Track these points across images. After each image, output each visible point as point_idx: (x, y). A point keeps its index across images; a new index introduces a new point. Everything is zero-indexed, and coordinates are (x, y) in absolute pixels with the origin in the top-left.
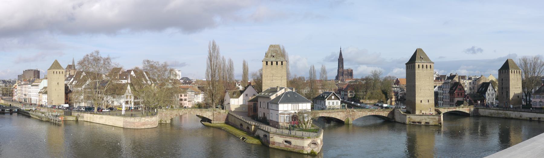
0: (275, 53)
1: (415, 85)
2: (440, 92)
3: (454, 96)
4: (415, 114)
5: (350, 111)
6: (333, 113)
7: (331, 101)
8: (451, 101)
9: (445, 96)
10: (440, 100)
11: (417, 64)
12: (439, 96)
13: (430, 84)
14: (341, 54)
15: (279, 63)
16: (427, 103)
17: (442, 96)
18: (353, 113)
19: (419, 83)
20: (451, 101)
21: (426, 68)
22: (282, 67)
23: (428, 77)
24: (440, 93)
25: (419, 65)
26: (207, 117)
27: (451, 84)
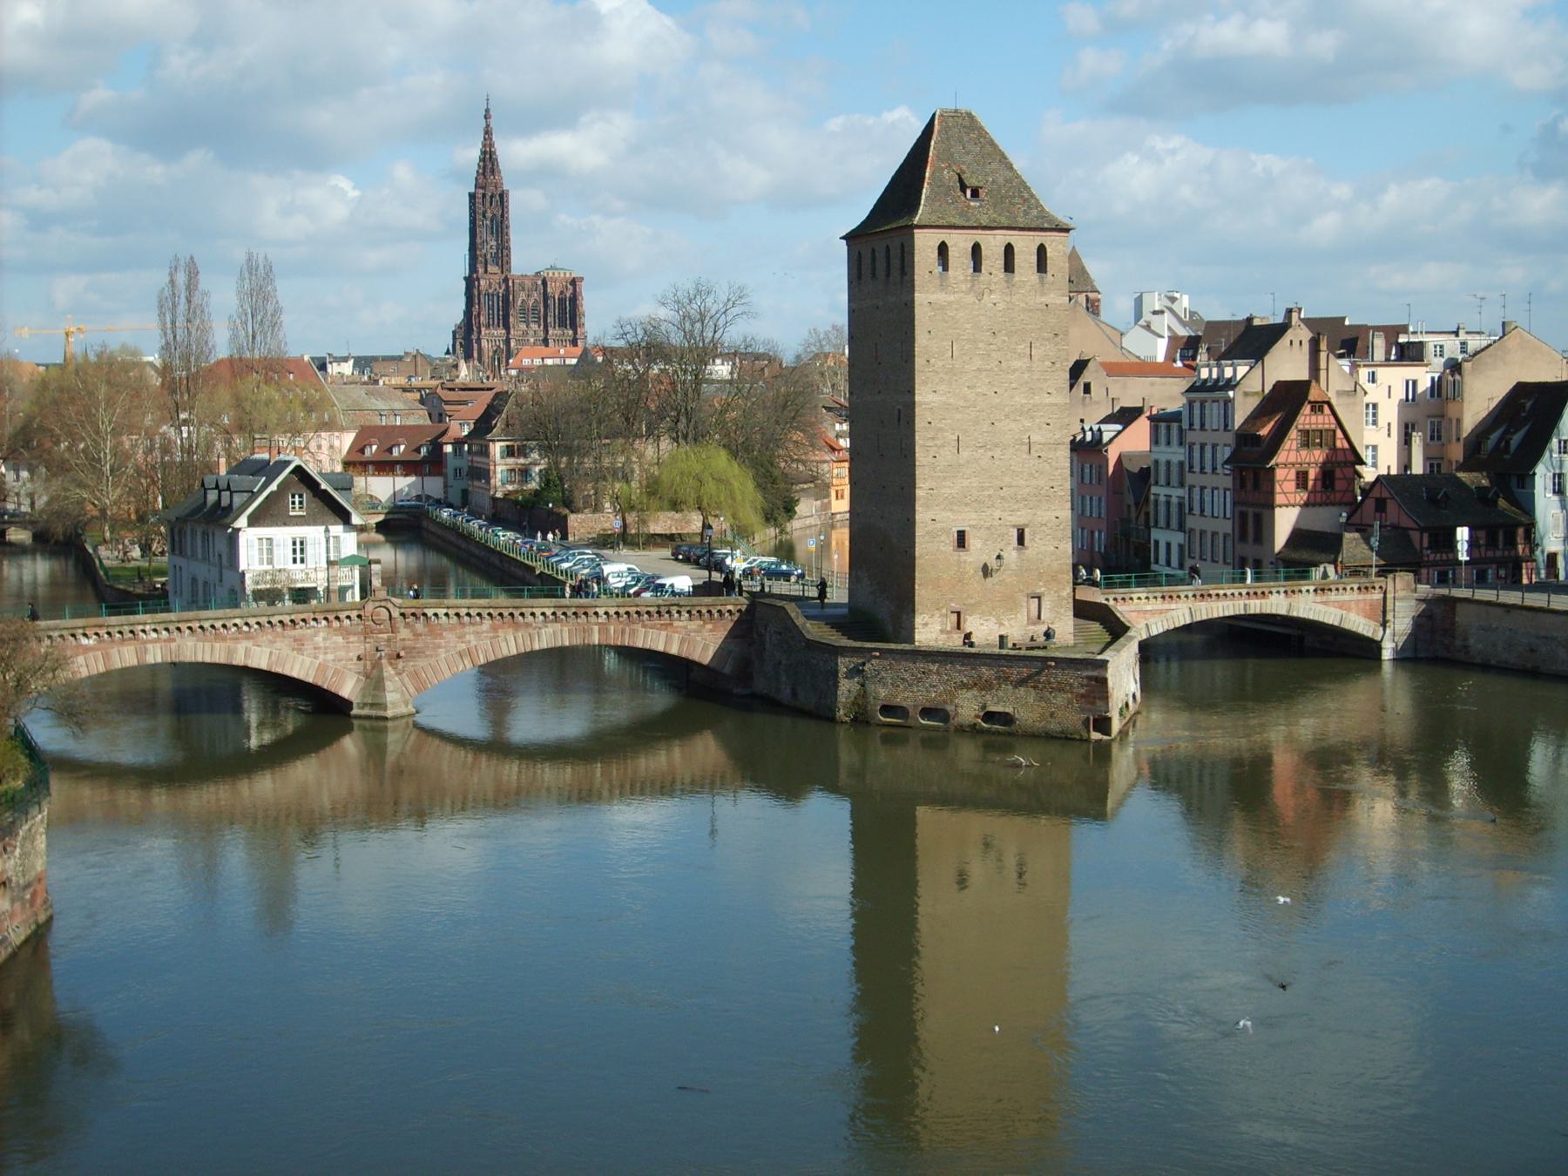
1: (911, 405)
2: (1163, 459)
3: (1272, 493)
4: (911, 640)
5: (396, 613)
7: (283, 535)
9: (1202, 488)
10: (1162, 522)
11: (925, 243)
12: (1154, 490)
14: (488, 162)
16: (1011, 554)
17: (1181, 492)
19: (942, 388)
20: (1243, 537)
21: (1001, 275)
23: (1023, 348)
24: (1162, 468)
25: (943, 249)
27: (1246, 394)
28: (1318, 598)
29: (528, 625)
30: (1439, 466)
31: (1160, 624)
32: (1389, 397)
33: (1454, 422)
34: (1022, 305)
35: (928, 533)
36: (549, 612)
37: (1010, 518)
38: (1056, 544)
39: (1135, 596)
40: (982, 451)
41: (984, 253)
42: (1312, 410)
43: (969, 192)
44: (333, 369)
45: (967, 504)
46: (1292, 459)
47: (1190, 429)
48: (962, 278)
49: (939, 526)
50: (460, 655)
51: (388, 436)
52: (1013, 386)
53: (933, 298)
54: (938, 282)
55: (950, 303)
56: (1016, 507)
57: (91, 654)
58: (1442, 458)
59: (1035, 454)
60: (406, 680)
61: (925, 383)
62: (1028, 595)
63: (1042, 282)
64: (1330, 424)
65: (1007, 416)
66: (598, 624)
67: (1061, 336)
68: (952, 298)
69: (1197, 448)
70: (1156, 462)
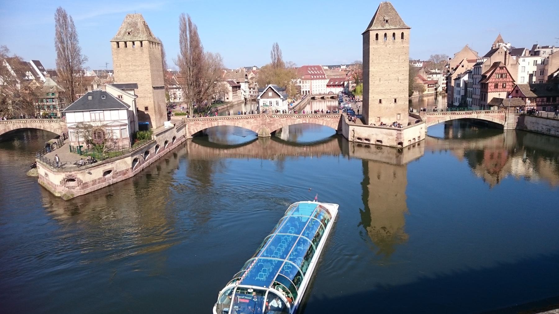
0: (133, 27)
1: (369, 71)
3: (487, 89)
5: (266, 116)
6: (241, 121)
8: (482, 99)
10: (469, 97)
12: (468, 89)
13: (400, 69)
15: (137, 44)
16: (393, 104)
17: (472, 89)
18: (271, 121)
20: (482, 99)
22: (142, 50)
23: (397, 57)
25: (377, 35)
26: (52, 131)
27: (485, 66)
28: (486, 115)
29: (294, 119)
30: (542, 81)
31: (442, 120)
32: (529, 65)
33: (546, 70)
34: (397, 47)
35: (372, 100)
36: (298, 116)
37: (393, 96)
38: (404, 102)
39: (435, 114)
40: (386, 81)
41: (387, 35)
42: (500, 69)
43: (385, 21)
44: (342, 67)
45: (382, 93)
46: (494, 81)
47: (474, 74)
48: (382, 42)
49: (375, 98)
50: (280, 125)
51: (335, 80)
52: (394, 66)
53: (374, 47)
54: (375, 43)
55: (378, 48)
56: (394, 94)
57: (209, 124)
58: (543, 80)
59: (399, 82)
60: (269, 129)
61: (372, 66)
62: (397, 114)
63: (402, 41)
64: (505, 72)
65: (392, 73)
66: (308, 119)
67: (407, 54)
68: (379, 46)
69: (475, 79)
70: (468, 82)
